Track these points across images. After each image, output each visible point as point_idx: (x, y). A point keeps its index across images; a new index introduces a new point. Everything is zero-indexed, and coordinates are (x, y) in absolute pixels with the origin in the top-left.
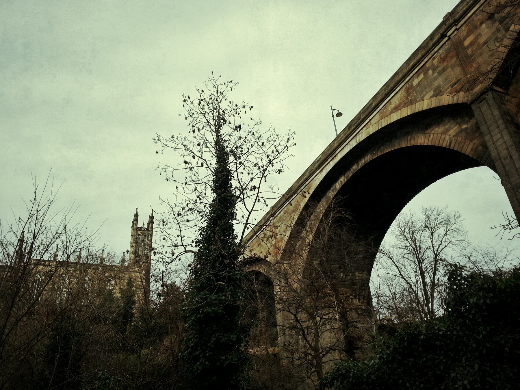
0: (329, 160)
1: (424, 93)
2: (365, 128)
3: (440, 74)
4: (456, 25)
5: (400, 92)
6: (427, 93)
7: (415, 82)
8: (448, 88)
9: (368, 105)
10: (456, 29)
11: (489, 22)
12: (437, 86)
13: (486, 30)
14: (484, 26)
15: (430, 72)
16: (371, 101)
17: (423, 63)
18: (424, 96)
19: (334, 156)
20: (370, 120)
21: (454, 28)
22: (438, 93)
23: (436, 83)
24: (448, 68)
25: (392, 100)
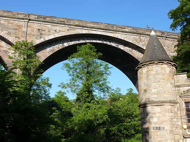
1: (4, 29)
3: (14, 29)
4: (29, 21)
6: (5, 30)
11: (38, 30)
14: (36, 29)
15: (11, 25)
21: (28, 21)
22: (9, 34)
23: (10, 31)
24: (18, 30)
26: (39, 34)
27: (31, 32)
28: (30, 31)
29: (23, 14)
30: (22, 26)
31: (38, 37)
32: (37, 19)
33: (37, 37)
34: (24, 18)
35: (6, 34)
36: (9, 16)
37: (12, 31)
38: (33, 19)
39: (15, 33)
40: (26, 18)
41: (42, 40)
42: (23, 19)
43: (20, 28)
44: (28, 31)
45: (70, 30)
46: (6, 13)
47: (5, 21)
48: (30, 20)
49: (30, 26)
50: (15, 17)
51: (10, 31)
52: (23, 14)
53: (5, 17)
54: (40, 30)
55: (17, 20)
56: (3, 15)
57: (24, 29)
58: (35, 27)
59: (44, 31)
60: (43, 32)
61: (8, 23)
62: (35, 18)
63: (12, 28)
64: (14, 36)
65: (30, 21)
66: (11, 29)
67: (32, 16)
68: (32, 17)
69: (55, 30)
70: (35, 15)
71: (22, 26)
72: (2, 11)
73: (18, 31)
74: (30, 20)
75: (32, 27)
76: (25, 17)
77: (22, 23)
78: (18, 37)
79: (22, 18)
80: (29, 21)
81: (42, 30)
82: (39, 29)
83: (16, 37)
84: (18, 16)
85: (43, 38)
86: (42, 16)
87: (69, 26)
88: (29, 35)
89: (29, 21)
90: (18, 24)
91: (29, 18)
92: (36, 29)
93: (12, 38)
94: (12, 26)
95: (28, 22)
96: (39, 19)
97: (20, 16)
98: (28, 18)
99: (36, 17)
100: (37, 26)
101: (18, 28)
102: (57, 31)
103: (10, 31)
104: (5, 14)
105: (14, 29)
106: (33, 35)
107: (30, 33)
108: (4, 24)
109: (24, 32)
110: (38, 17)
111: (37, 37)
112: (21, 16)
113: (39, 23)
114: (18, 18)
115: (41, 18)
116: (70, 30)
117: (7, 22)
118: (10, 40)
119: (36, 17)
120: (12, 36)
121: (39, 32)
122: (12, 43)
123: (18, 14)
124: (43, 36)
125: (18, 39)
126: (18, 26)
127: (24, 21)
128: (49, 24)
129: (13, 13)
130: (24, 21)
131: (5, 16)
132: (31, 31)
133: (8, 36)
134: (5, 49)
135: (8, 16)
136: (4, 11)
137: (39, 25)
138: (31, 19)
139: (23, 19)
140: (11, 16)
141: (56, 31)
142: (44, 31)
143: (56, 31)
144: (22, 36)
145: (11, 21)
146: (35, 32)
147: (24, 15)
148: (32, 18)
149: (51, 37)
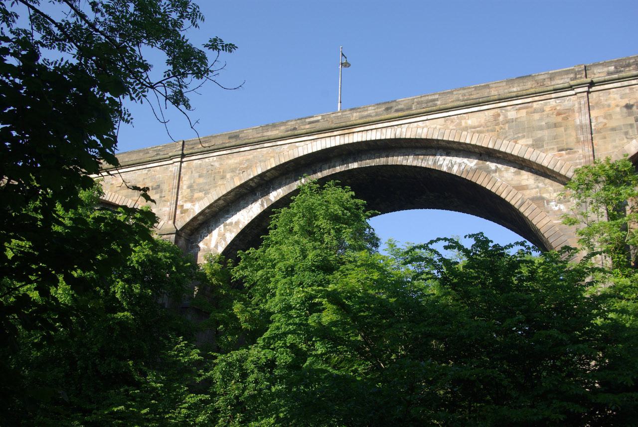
0: (335, 133)
1: (520, 135)
3: (549, 126)
4: (590, 87)
5: (486, 112)
6: (524, 137)
11: (625, 110)
12: (540, 138)
13: (619, 117)
14: (618, 109)
15: (536, 116)
19: (347, 131)
21: (586, 89)
22: (538, 144)
23: (539, 134)
24: (561, 126)
27: (605, 121)
28: (601, 120)
29: (567, 72)
30: (571, 110)
31: (630, 131)
32: (616, 76)
33: (626, 133)
34: (572, 83)
35: (528, 146)
36: (528, 92)
37: (545, 134)
38: (602, 79)
39: (555, 138)
40: (578, 81)
42: (571, 88)
43: (566, 119)
44: (593, 120)
46: (516, 85)
47: (520, 109)
48: (592, 84)
49: (598, 105)
50: (545, 89)
51: (539, 134)
52: (567, 72)
53: (517, 97)
55: (553, 96)
56: (509, 95)
57: (581, 119)
58: (613, 103)
61: (527, 113)
62: (609, 73)
63: (544, 123)
64: (553, 149)
65: (594, 89)
66: (541, 128)
67: (596, 70)
68: (598, 74)
70: (605, 64)
71: (573, 111)
72: (504, 84)
73: (562, 129)
74: (592, 84)
75: (603, 106)
76: (575, 78)
77: (572, 101)
78: (566, 147)
79: (566, 85)
80: (591, 90)
83: (562, 150)
84: (553, 83)
86: (632, 61)
88: (599, 132)
89: (591, 90)
90: (558, 108)
91: (589, 80)
92: (618, 109)
93: (550, 154)
94: (541, 119)
95: (588, 92)
96: (621, 72)
97: (559, 82)
98: (584, 80)
99: (612, 68)
100: (621, 98)
101: (559, 119)
103: (539, 136)
104: (515, 89)
105: (549, 126)
106: (613, 129)
107: (600, 126)
108: (516, 119)
109: (582, 127)
110: (616, 68)
111: (626, 133)
112: (562, 81)
113: (626, 83)
114: (556, 90)
115: (628, 65)
117: (523, 113)
118: (545, 164)
119: (612, 68)
120: (548, 148)
121: (630, 114)
122: (552, 171)
123: (551, 78)
125: (569, 153)
126: (559, 114)
127: (576, 94)
129: (537, 78)
130: (573, 92)
131: (514, 94)
132: (605, 118)
133: (537, 152)
134: (533, 193)
135: (524, 92)
136: (510, 82)
137: (627, 90)
138: (595, 80)
139: (571, 87)
140: (533, 91)
144: (578, 141)
145: (535, 105)
147: (572, 76)
148: (597, 76)
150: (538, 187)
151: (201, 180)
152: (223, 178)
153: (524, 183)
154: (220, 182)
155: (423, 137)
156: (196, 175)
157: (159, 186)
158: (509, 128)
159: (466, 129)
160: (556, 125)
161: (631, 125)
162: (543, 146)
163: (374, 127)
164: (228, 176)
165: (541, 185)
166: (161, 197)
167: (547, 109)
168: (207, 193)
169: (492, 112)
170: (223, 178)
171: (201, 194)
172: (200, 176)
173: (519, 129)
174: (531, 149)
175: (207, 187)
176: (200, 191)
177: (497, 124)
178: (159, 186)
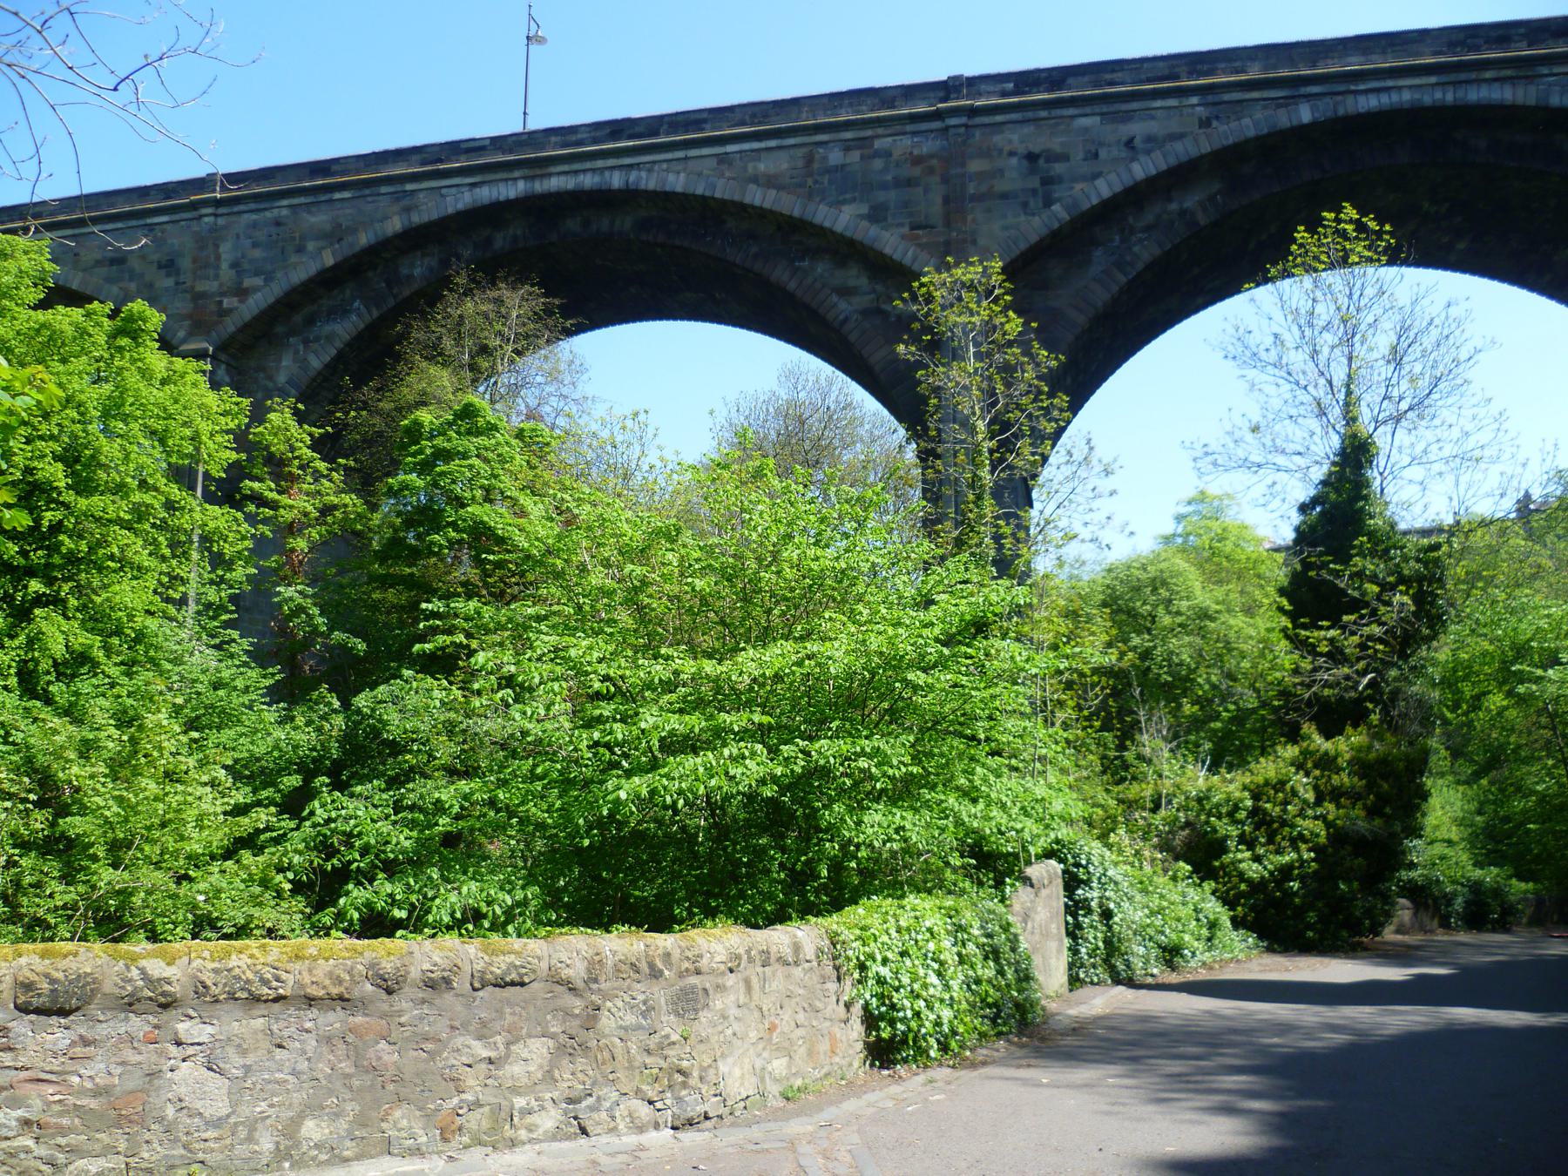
0: (517, 174)
1: (848, 196)
2: (665, 166)
3: (898, 183)
6: (854, 200)
7: (835, 157)
8: (902, 225)
9: (693, 117)
10: (966, 126)
11: (1025, 163)
14: (1014, 161)
15: (878, 164)
16: (705, 115)
17: (869, 133)
18: (844, 202)
19: (538, 172)
20: (686, 158)
22: (877, 215)
23: (881, 196)
24: (918, 185)
25: (763, 155)
26: (1035, 182)
31: (1032, 203)
33: (1025, 205)
35: (862, 217)
37: (892, 196)
41: (1060, 212)
45: (1215, 124)
51: (881, 196)
54: (1041, 161)
55: (909, 128)
59: (1064, 157)
60: (1059, 168)
61: (862, 157)
63: (889, 178)
66: (884, 186)
69: (1124, 139)
73: (920, 190)
81: (1053, 157)
82: (1031, 157)
83: (919, 228)
85: (1058, 200)
87: (1210, 98)
94: (886, 170)
101: (917, 171)
102: (1137, 142)
105: (898, 183)
106: (1004, 196)
108: (843, 166)
111: (1025, 205)
113: (1030, 115)
116: (1215, 124)
117: (855, 156)
121: (1033, 171)
124: (1058, 191)
128: (1088, 110)
141: (1129, 143)
142: (1064, 157)
143: (1129, 143)
146: (1013, 177)
149: (1104, 188)
150: (874, 291)
151: (257, 253)
152: (300, 250)
153: (852, 282)
154: (294, 259)
155: (679, 189)
156: (248, 242)
157: (172, 261)
158: (830, 182)
159: (755, 179)
160: (910, 182)
161: (1034, 192)
162: (885, 219)
163: (588, 165)
164: (311, 246)
165: (879, 288)
166: (177, 283)
167: (896, 154)
168: (269, 279)
169: (800, 152)
170: (300, 250)
171: (258, 281)
172: (255, 245)
173: (845, 185)
174: (865, 223)
175: (269, 267)
176: (256, 274)
177: (811, 174)
178: (172, 261)
